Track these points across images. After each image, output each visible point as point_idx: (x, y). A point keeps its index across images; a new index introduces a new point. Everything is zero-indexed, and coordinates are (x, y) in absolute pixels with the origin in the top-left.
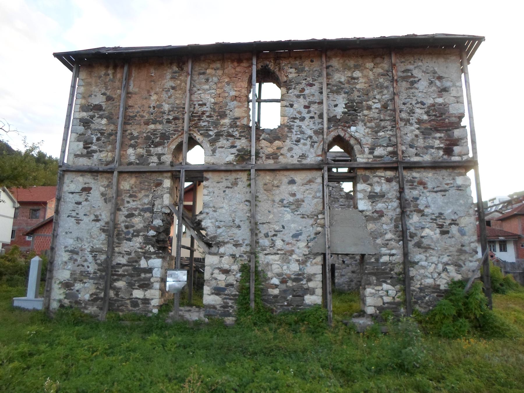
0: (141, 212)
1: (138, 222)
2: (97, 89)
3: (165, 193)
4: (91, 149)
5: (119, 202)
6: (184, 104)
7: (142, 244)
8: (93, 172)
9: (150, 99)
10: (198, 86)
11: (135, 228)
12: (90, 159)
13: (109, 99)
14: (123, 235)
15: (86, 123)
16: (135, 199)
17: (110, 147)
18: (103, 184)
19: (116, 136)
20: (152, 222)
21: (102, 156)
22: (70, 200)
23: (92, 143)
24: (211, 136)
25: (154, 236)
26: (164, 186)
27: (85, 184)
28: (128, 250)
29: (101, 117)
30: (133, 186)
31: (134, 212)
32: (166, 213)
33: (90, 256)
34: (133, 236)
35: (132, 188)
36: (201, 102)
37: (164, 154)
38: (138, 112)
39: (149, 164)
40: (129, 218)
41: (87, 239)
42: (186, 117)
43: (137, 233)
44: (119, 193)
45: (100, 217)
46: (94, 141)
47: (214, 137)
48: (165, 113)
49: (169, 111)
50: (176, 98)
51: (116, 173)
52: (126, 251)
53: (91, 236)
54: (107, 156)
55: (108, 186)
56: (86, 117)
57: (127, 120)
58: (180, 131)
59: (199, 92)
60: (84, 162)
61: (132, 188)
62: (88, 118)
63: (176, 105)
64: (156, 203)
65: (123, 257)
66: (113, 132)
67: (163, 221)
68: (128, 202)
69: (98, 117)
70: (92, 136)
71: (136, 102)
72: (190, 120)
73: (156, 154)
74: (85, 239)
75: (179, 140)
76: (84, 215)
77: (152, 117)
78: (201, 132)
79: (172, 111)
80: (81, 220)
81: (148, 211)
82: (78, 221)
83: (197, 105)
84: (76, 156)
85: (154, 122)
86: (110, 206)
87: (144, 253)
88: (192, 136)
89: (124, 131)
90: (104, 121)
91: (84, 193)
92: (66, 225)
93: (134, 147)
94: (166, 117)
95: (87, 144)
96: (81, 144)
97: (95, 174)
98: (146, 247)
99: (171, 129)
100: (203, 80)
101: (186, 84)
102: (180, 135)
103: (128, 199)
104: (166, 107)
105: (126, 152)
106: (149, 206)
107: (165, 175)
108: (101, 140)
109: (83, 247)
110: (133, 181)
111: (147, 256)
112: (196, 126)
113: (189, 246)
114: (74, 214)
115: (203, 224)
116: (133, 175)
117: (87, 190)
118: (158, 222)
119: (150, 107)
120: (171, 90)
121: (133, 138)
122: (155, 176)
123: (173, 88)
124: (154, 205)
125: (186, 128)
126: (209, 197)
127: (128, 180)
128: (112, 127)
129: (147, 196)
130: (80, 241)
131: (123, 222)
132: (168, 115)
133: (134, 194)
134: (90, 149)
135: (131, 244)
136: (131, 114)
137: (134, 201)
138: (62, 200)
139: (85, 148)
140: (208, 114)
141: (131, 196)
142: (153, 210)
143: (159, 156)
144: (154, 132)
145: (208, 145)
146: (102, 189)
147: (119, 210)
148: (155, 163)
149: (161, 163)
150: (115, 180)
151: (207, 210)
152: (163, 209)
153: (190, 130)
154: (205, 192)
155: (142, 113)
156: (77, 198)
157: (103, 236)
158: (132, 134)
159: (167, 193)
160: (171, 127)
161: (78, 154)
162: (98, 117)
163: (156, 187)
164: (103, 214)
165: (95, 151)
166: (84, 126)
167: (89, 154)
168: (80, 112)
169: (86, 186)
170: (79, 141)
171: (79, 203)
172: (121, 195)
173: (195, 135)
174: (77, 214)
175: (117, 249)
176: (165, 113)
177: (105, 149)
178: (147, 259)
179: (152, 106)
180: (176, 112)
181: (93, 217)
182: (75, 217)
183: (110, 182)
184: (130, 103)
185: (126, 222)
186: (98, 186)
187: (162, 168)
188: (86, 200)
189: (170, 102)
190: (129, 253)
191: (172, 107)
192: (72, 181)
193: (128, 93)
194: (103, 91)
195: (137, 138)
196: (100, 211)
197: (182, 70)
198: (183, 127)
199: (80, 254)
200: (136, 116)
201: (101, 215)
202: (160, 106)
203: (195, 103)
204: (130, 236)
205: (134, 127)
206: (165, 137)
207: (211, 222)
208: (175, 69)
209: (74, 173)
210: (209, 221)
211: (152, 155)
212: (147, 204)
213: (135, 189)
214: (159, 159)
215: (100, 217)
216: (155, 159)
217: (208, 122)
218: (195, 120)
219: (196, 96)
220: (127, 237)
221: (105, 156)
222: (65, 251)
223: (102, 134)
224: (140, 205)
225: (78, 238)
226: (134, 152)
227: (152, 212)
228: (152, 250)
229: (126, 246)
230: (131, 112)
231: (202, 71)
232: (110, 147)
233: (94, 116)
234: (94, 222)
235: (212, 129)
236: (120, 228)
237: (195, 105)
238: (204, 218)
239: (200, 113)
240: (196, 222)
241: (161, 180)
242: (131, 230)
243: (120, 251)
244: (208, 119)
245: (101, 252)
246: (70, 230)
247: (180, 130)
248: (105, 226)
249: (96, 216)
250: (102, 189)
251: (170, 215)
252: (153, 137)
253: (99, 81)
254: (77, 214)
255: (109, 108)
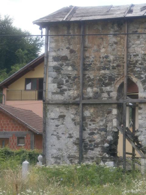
0: (99, 131)
1: (97, 138)
2: (63, 45)
3: (113, 119)
4: (63, 88)
5: (84, 125)
6: (124, 55)
7: (100, 152)
8: (66, 104)
9: (100, 51)
10: (132, 42)
11: (95, 142)
12: (62, 95)
13: (72, 51)
14: (88, 147)
15: (58, 70)
16: (94, 123)
17: (75, 87)
18: (72, 112)
19: (79, 79)
20: (106, 138)
21: (70, 93)
22: (52, 124)
23: (63, 84)
24: (142, 78)
25: (107, 147)
26: (113, 113)
27: (61, 113)
28: (92, 156)
29: (68, 65)
30: (93, 114)
31: (94, 131)
32: (115, 132)
33: (69, 160)
34: (95, 147)
35: (92, 115)
36: (135, 54)
37: (112, 92)
38: (92, 61)
39: (102, 98)
40: (91, 135)
41: (65, 149)
42: (125, 65)
43: (97, 145)
44: (84, 118)
45: (72, 135)
46: (64, 83)
47: (144, 79)
48: (111, 62)
49: (114, 60)
50: (118, 51)
51: (81, 105)
52: (90, 157)
53: (68, 148)
54: (74, 93)
55: (76, 114)
56: (57, 65)
57: (85, 68)
58: (122, 75)
59: (134, 46)
60: (59, 98)
61: (92, 115)
62: (59, 66)
63: (118, 56)
64: (108, 125)
65: (89, 160)
66: (77, 76)
67: (113, 137)
68: (90, 125)
69: (65, 65)
70: (63, 79)
71: (91, 55)
72: (128, 67)
73: (107, 92)
74: (64, 149)
75: (121, 81)
76: (63, 134)
77: (103, 65)
78: (136, 75)
79: (116, 60)
80: (60, 137)
81: (103, 131)
82: (59, 138)
83: (132, 56)
84: (53, 93)
85: (104, 69)
86: (78, 127)
87: (102, 158)
88: (130, 78)
89: (84, 75)
90: (70, 68)
91: (61, 119)
92: (51, 141)
93: (91, 86)
94: (111, 65)
95: (60, 85)
96: (56, 85)
97: (67, 106)
98: (103, 154)
99: (116, 73)
100: (136, 37)
101: (124, 40)
102: (122, 78)
103: (90, 123)
104: (111, 58)
105: (86, 90)
106: (104, 127)
107: (114, 106)
108: (69, 82)
109: (63, 155)
110: (92, 111)
111: (104, 159)
112: (132, 71)
113: (131, 152)
114: (55, 133)
115: (139, 138)
116: (92, 106)
117: (62, 117)
118: (110, 138)
119: (100, 58)
120: (114, 45)
121: (90, 80)
122: (106, 107)
123: (116, 43)
124: (107, 126)
125: (125, 74)
126: (143, 120)
127: (89, 110)
128: (76, 72)
129: (102, 120)
130: (60, 151)
131: (87, 138)
132: (113, 63)
133: (94, 119)
134: (62, 88)
135: (94, 152)
136: (88, 63)
137: (94, 124)
138: (47, 124)
139: (59, 88)
140: (140, 62)
141: (92, 121)
142: (106, 130)
143: (109, 93)
144: (104, 76)
145: (141, 85)
146: (73, 116)
147: (85, 130)
148: (106, 97)
149: (110, 98)
150: (80, 109)
151: (141, 130)
152: (113, 129)
153: (128, 74)
154: (140, 117)
155: (95, 62)
156: (57, 122)
157: (75, 147)
158: (89, 77)
159: (115, 118)
160: (115, 73)
161: (54, 92)
162: (65, 65)
163: (108, 114)
164: (74, 133)
165: (65, 90)
166: (56, 72)
167: (62, 92)
168: (53, 61)
169: (62, 114)
170: (54, 82)
171: (57, 126)
172: (85, 120)
173: (132, 77)
174: (58, 133)
175: (85, 156)
176: (111, 62)
177: (72, 89)
178: (104, 161)
179: (101, 56)
180: (118, 61)
181: (67, 135)
182: (56, 135)
183: (77, 111)
184: (87, 54)
185: (89, 138)
186: (70, 114)
187: (110, 101)
188: (62, 124)
189: (114, 54)
190: (92, 158)
191: (116, 58)
192: (52, 111)
193: (85, 47)
194: (67, 46)
195: (93, 80)
196: (72, 131)
197: (121, 29)
198: (124, 72)
199: (62, 159)
200: (91, 64)
201: (73, 134)
202: (107, 57)
203: (131, 54)
204: (93, 147)
205: (91, 73)
206: (112, 79)
207: (145, 137)
208: (116, 28)
209: (53, 105)
210: (143, 136)
211: (104, 92)
212: (103, 126)
213: (94, 116)
214: (109, 95)
215: (72, 135)
216: (105, 95)
217: (141, 68)
218: (131, 67)
219: (131, 49)
220: (91, 148)
221: (72, 93)
222: (52, 158)
223: (69, 77)
224: (98, 126)
225: (59, 149)
226: (92, 90)
227: (106, 131)
228: (107, 156)
229: (90, 154)
230: (87, 62)
231: (135, 30)
232: (75, 87)
233: (62, 65)
234: (68, 139)
235: (143, 73)
236: (86, 142)
237: (131, 55)
238: (140, 135)
239: (135, 61)
240: (135, 137)
241: (110, 109)
242: (93, 143)
243: (87, 157)
244: (140, 66)
245: (75, 158)
246: (54, 144)
247: (121, 74)
248: (76, 141)
249: (70, 134)
250: (73, 116)
251: (117, 133)
252: (104, 79)
253: (64, 38)
254: (58, 133)
255: (72, 59)
